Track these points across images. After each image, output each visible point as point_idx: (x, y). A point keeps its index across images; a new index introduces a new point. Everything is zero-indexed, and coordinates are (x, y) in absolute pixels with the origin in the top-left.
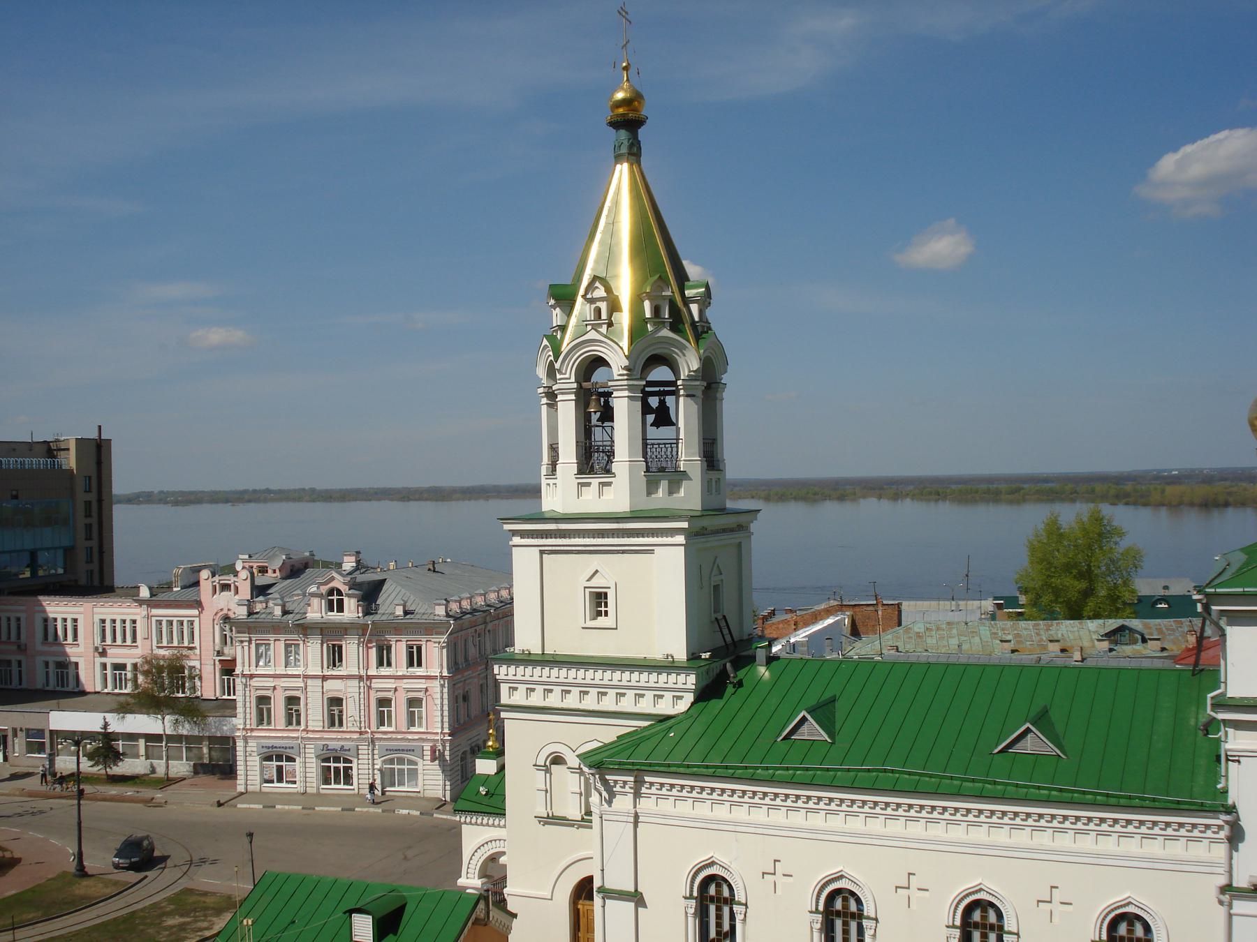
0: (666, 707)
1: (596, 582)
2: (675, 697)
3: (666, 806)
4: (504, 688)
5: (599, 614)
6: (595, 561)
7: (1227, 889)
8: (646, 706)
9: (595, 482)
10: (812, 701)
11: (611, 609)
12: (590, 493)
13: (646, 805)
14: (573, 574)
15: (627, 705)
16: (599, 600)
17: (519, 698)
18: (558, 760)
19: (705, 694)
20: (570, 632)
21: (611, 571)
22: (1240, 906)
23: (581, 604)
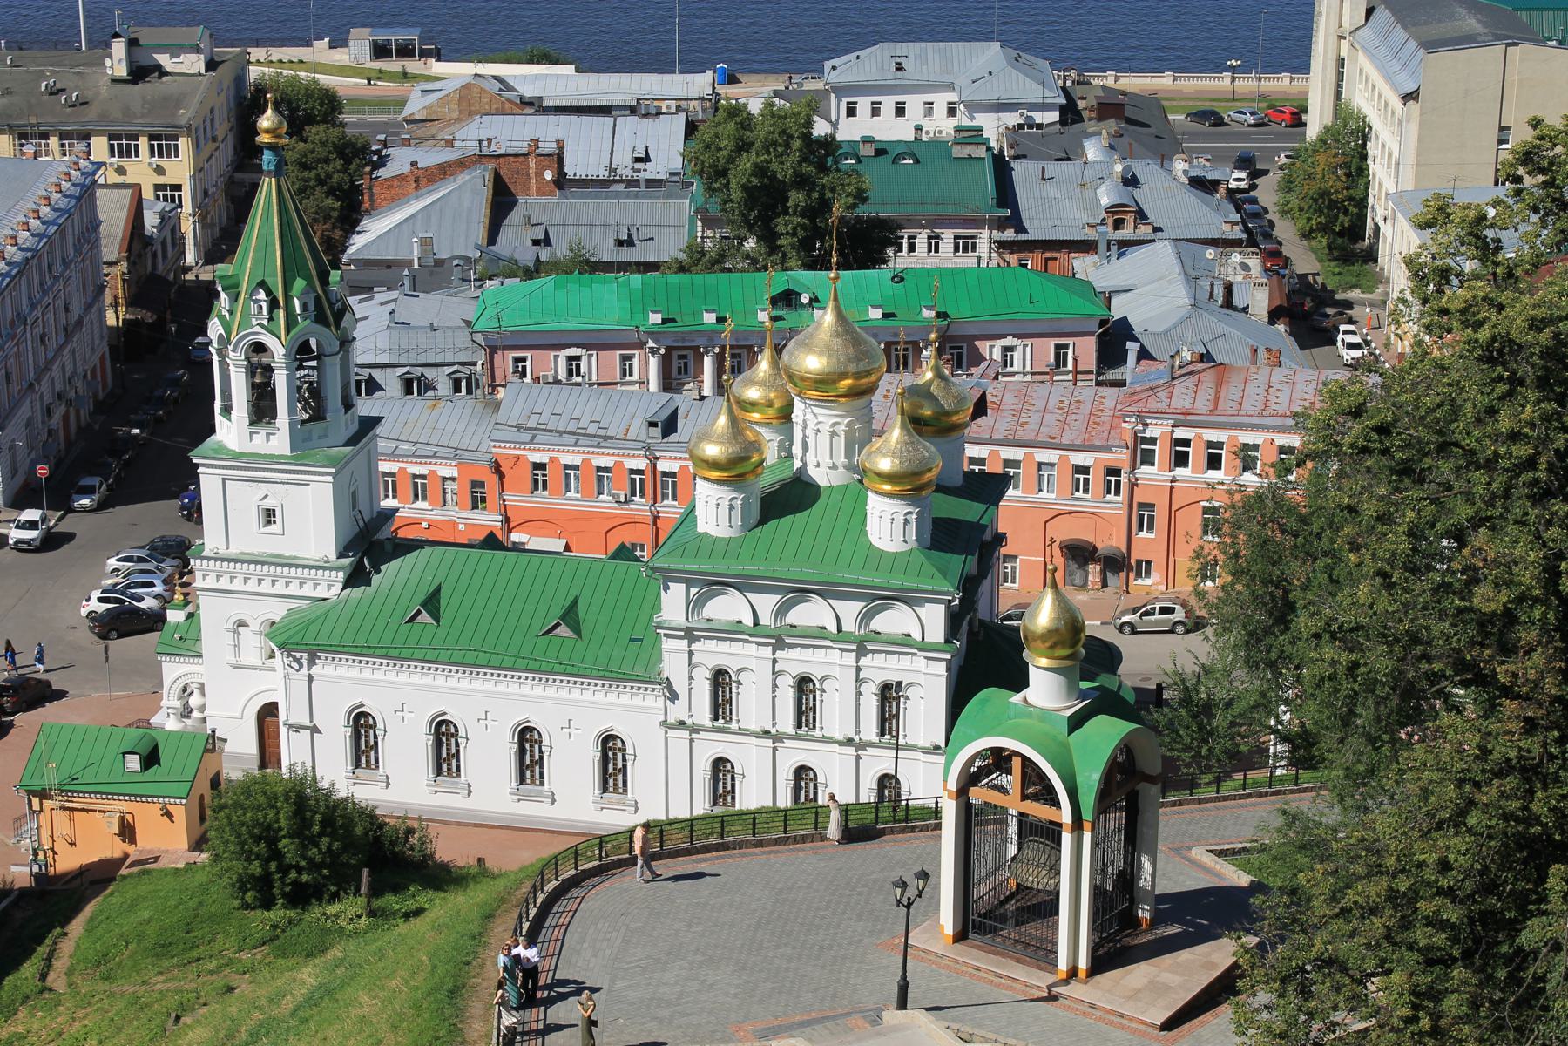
0: (321, 592)
1: (269, 503)
2: (330, 586)
3: (329, 670)
4: (198, 575)
5: (269, 522)
6: (264, 489)
7: (664, 724)
8: (307, 591)
9: (263, 432)
10: (422, 597)
11: (278, 518)
12: (259, 438)
13: (314, 670)
14: (247, 498)
15: (293, 589)
16: (269, 516)
17: (210, 582)
18: (242, 624)
19: (350, 583)
20: (249, 537)
21: (277, 496)
22: (671, 733)
23: (254, 517)
